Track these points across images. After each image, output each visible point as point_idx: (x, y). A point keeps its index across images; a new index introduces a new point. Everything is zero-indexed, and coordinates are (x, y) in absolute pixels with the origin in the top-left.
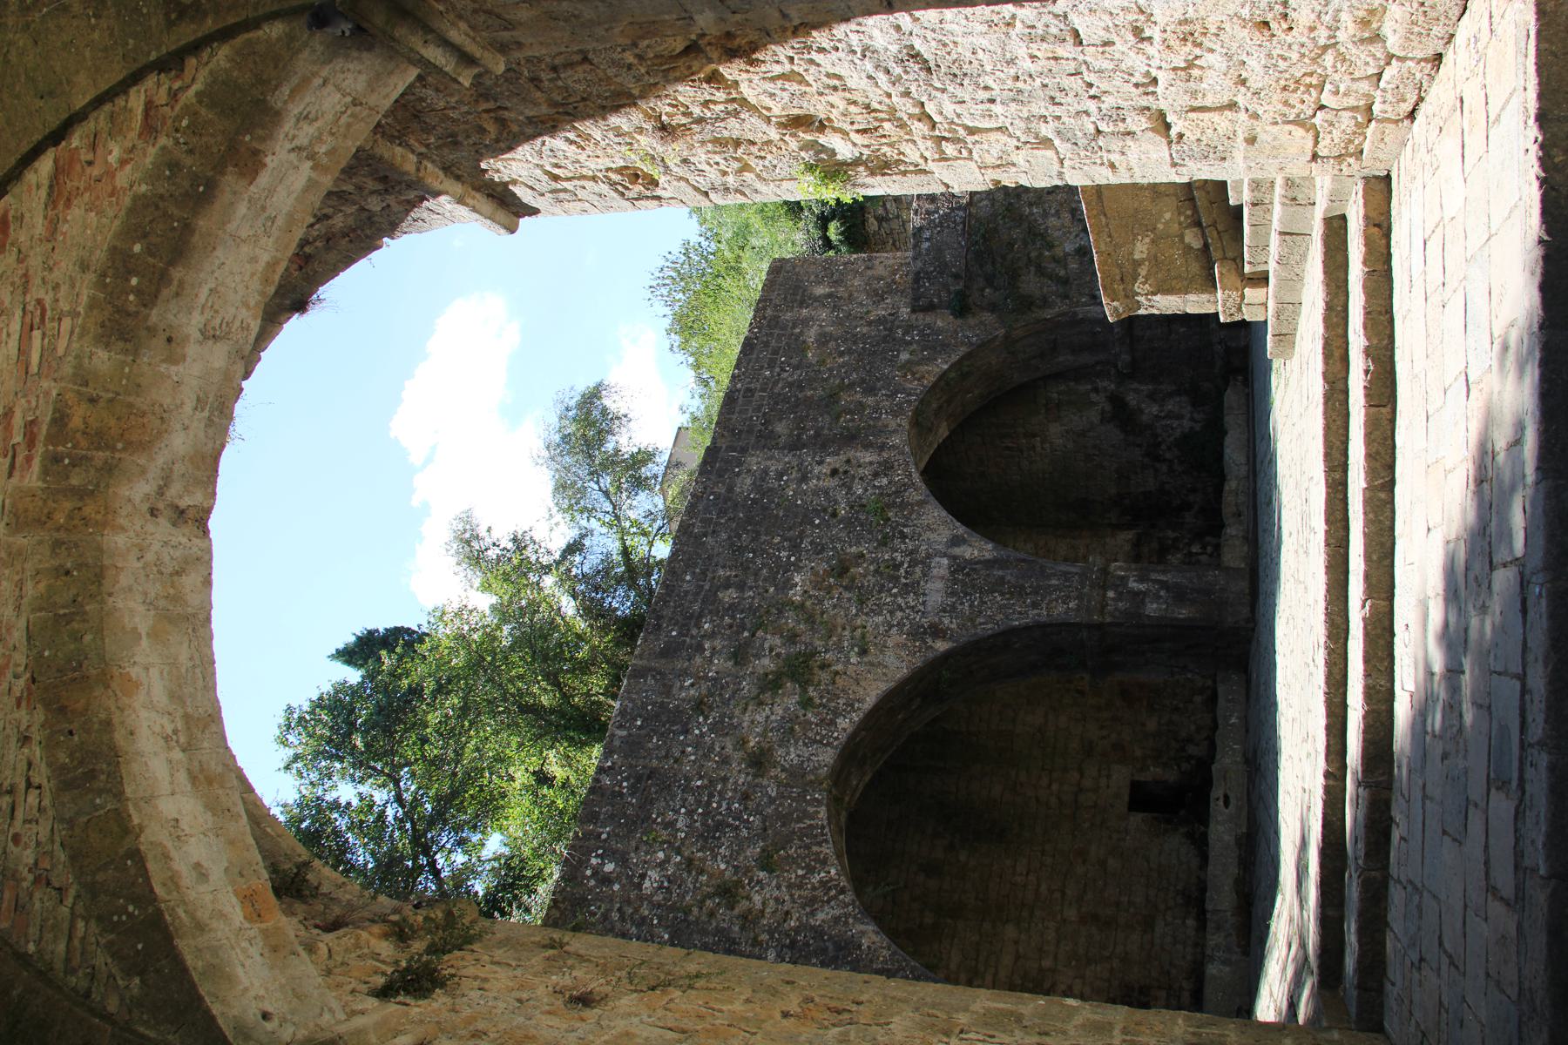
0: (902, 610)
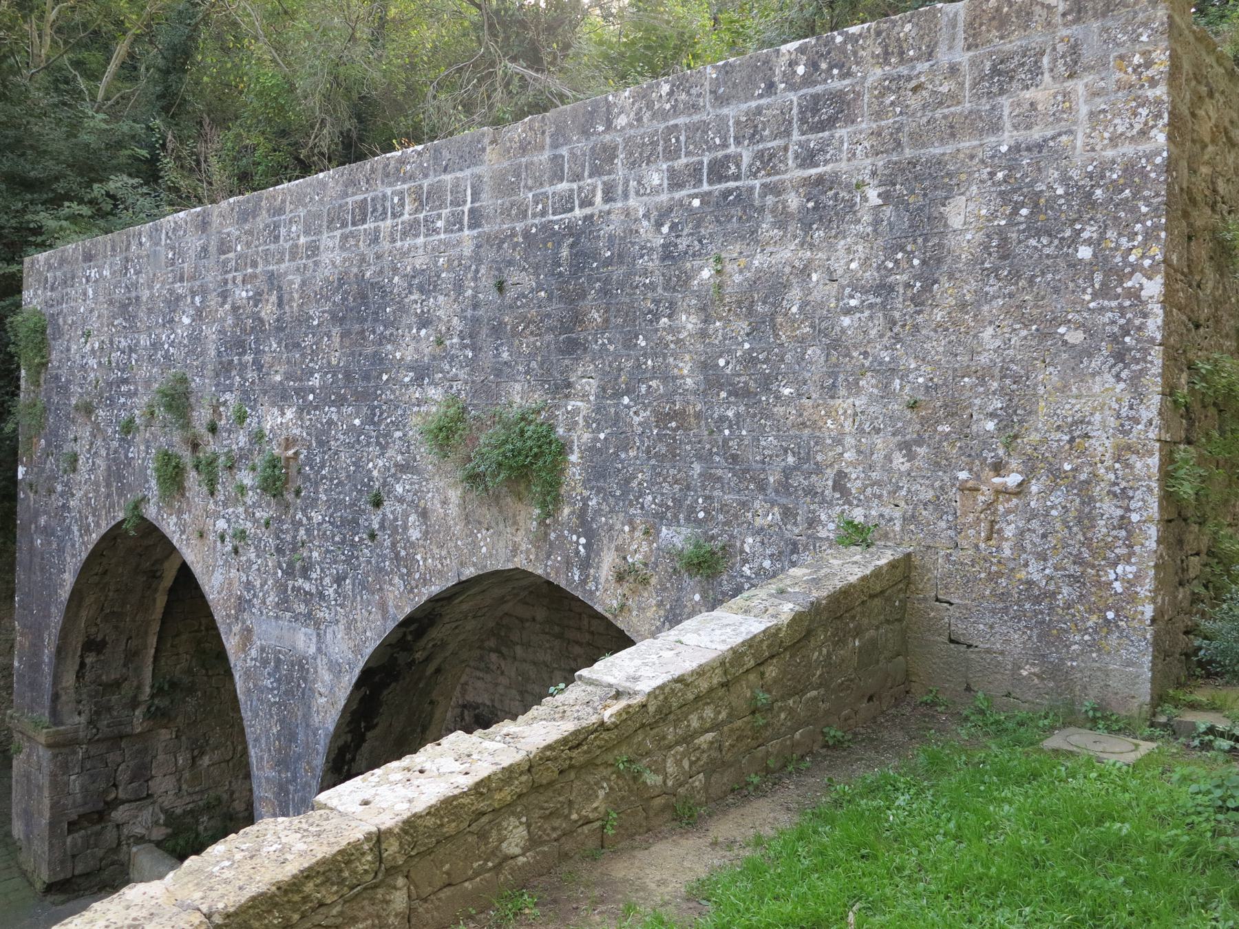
0: (262, 586)
